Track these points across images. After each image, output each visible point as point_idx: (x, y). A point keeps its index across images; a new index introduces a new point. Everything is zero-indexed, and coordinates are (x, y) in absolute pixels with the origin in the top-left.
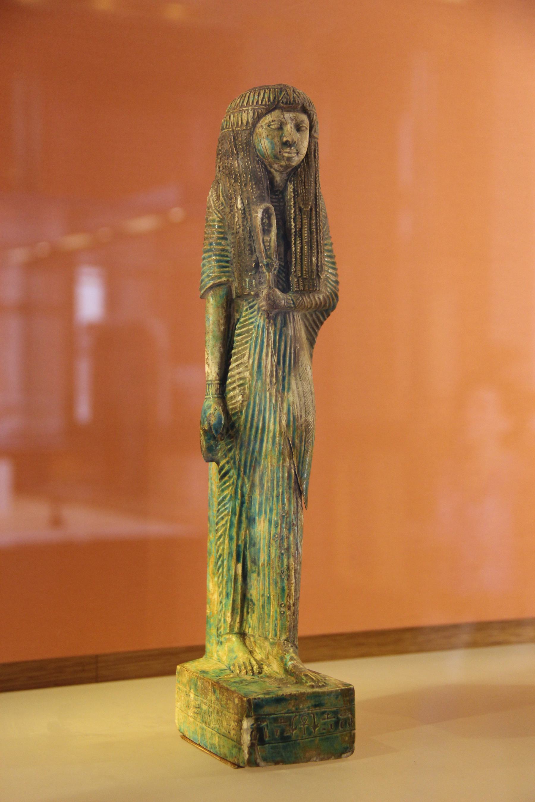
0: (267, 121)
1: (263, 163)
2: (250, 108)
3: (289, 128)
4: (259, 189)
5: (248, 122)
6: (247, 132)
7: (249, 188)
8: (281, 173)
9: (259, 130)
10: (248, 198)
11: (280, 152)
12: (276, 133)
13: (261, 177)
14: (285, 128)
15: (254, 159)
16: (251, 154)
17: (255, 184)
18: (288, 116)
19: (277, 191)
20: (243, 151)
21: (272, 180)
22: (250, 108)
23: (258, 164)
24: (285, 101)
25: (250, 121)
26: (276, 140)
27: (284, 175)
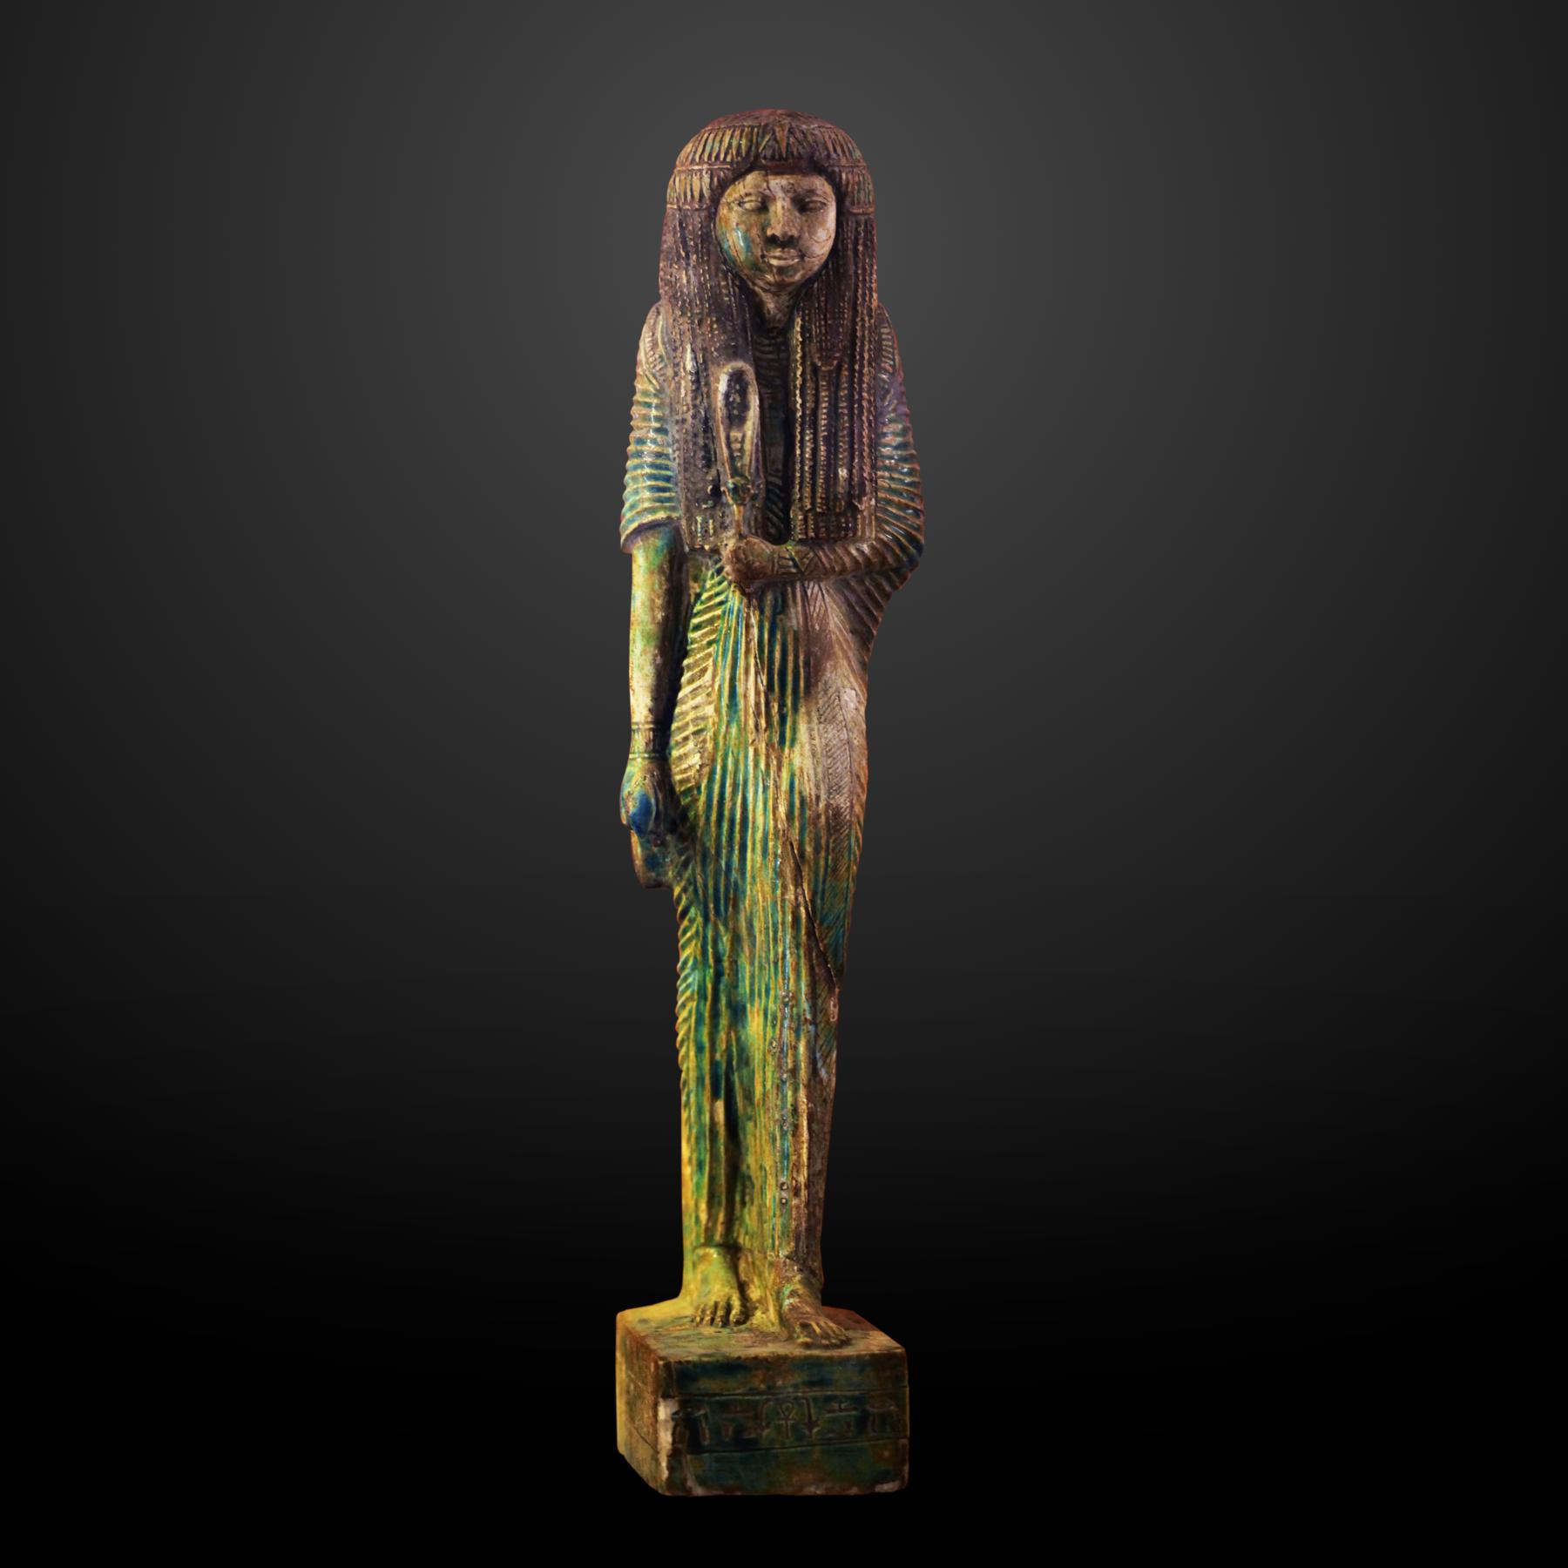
0: (736, 195)
1: (736, 276)
2: (705, 167)
3: (780, 207)
4: (725, 332)
5: (701, 195)
6: (703, 214)
7: (706, 329)
8: (775, 294)
9: (723, 211)
10: (704, 350)
11: (763, 256)
12: (754, 218)
13: (730, 306)
14: (772, 209)
15: (717, 269)
16: (713, 258)
17: (717, 321)
18: (777, 183)
19: (771, 330)
20: (697, 252)
21: (758, 308)
22: (705, 167)
23: (726, 278)
24: (769, 153)
25: (706, 193)
26: (755, 232)
27: (784, 298)
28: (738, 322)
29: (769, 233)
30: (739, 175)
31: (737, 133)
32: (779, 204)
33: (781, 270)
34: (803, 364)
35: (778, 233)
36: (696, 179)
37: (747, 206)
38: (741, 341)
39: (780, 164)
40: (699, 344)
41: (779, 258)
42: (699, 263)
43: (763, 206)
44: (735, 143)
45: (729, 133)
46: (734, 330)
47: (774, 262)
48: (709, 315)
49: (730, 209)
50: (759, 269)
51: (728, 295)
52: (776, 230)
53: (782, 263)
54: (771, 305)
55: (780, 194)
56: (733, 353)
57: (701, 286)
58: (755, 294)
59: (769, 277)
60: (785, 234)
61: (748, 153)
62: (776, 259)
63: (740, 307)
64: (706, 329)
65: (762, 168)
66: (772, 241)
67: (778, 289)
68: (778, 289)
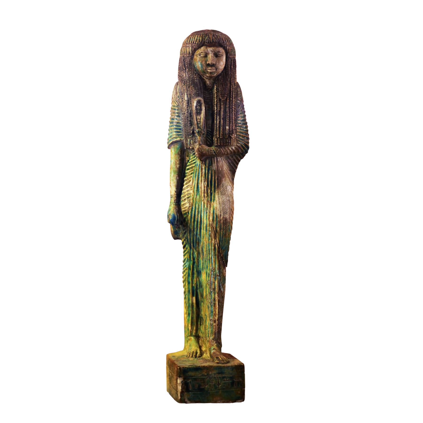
0: (199, 53)
1: (199, 74)
2: (190, 45)
3: (211, 56)
4: (195, 90)
5: (189, 53)
6: (190, 58)
7: (190, 89)
8: (209, 79)
9: (195, 57)
10: (190, 94)
11: (206, 69)
12: (203, 59)
13: (197, 83)
14: (208, 56)
15: (194, 73)
16: (192, 70)
17: (194, 87)
18: (210, 49)
19: (208, 89)
20: (188, 68)
21: (204, 83)
22: (190, 45)
23: (196, 75)
24: (207, 41)
25: (191, 52)
26: (204, 62)
27: (212, 80)
28: (199, 87)
29: (207, 63)
30: (199, 47)
31: (199, 36)
32: (210, 55)
33: (211, 73)
34: (217, 98)
35: (210, 63)
36: (188, 48)
37: (202, 56)
38: (200, 92)
39: (210, 44)
40: (189, 93)
41: (210, 70)
42: (189, 71)
43: (206, 56)
44: (198, 39)
45: (197, 36)
46: (198, 89)
47: (209, 71)
48: (191, 85)
49: (197, 56)
50: (205, 73)
51: (196, 80)
52: (209, 62)
53: (211, 71)
54: (208, 82)
55: (210, 52)
56: (198, 95)
57: (189, 77)
58: (204, 79)
59: (208, 75)
60: (212, 63)
61: (202, 41)
62: (209, 70)
63: (200, 83)
64: (190, 89)
65: (206, 45)
66: (208, 65)
67: (210, 78)
68: (210, 78)
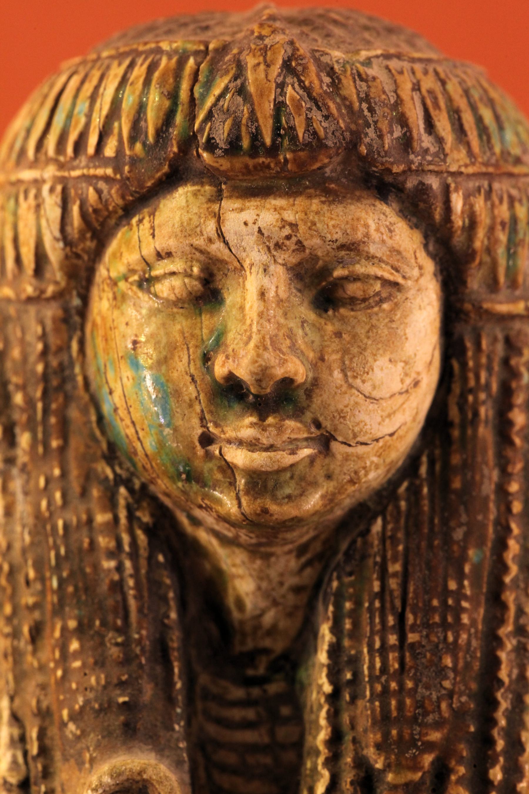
0: (131, 258)
1: (143, 495)
2: (50, 172)
3: (257, 292)
4: (100, 663)
5: (40, 258)
6: (51, 312)
7: (49, 653)
8: (254, 551)
9: (101, 304)
10: (44, 714)
11: (207, 440)
12: (181, 324)
13: (118, 587)
14: (231, 298)
15: (88, 477)
16: (76, 443)
17: (81, 631)
18: (247, 221)
19: (252, 657)
20: (31, 425)
21: (205, 592)
22: (50, 172)
23: (111, 503)
24: (222, 132)
25: (54, 252)
26: (183, 365)
27: (285, 563)
28: (141, 633)
29: (220, 370)
30: (141, 199)
31: (139, 71)
32: (253, 282)
33: (260, 482)
34: (333, 761)
35: (243, 372)
36: (26, 207)
37: (163, 289)
38: (148, 691)
39: (262, 163)
40: (31, 699)
41: (252, 445)
42: (42, 454)
43: (207, 292)
44: (129, 101)
45: (117, 71)
46: (127, 660)
47: (238, 457)
48: (59, 610)
49: (118, 300)
50: (193, 476)
51: (115, 553)
52: (239, 362)
53: (259, 459)
54: (244, 582)
55: (254, 255)
56: (130, 727)
57: (41, 523)
58: (196, 549)
59: (228, 503)
60: (262, 374)
61: (162, 132)
62: (243, 443)
63: (151, 589)
64: (49, 653)
65: (210, 176)
66: (231, 391)
67: (262, 534)
68: (262, 534)
